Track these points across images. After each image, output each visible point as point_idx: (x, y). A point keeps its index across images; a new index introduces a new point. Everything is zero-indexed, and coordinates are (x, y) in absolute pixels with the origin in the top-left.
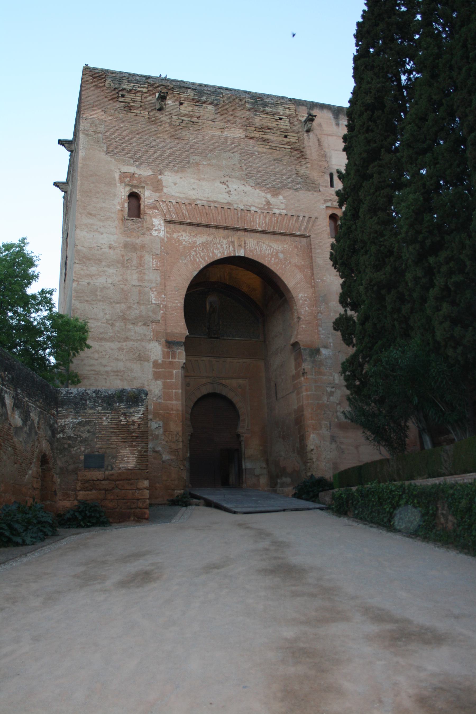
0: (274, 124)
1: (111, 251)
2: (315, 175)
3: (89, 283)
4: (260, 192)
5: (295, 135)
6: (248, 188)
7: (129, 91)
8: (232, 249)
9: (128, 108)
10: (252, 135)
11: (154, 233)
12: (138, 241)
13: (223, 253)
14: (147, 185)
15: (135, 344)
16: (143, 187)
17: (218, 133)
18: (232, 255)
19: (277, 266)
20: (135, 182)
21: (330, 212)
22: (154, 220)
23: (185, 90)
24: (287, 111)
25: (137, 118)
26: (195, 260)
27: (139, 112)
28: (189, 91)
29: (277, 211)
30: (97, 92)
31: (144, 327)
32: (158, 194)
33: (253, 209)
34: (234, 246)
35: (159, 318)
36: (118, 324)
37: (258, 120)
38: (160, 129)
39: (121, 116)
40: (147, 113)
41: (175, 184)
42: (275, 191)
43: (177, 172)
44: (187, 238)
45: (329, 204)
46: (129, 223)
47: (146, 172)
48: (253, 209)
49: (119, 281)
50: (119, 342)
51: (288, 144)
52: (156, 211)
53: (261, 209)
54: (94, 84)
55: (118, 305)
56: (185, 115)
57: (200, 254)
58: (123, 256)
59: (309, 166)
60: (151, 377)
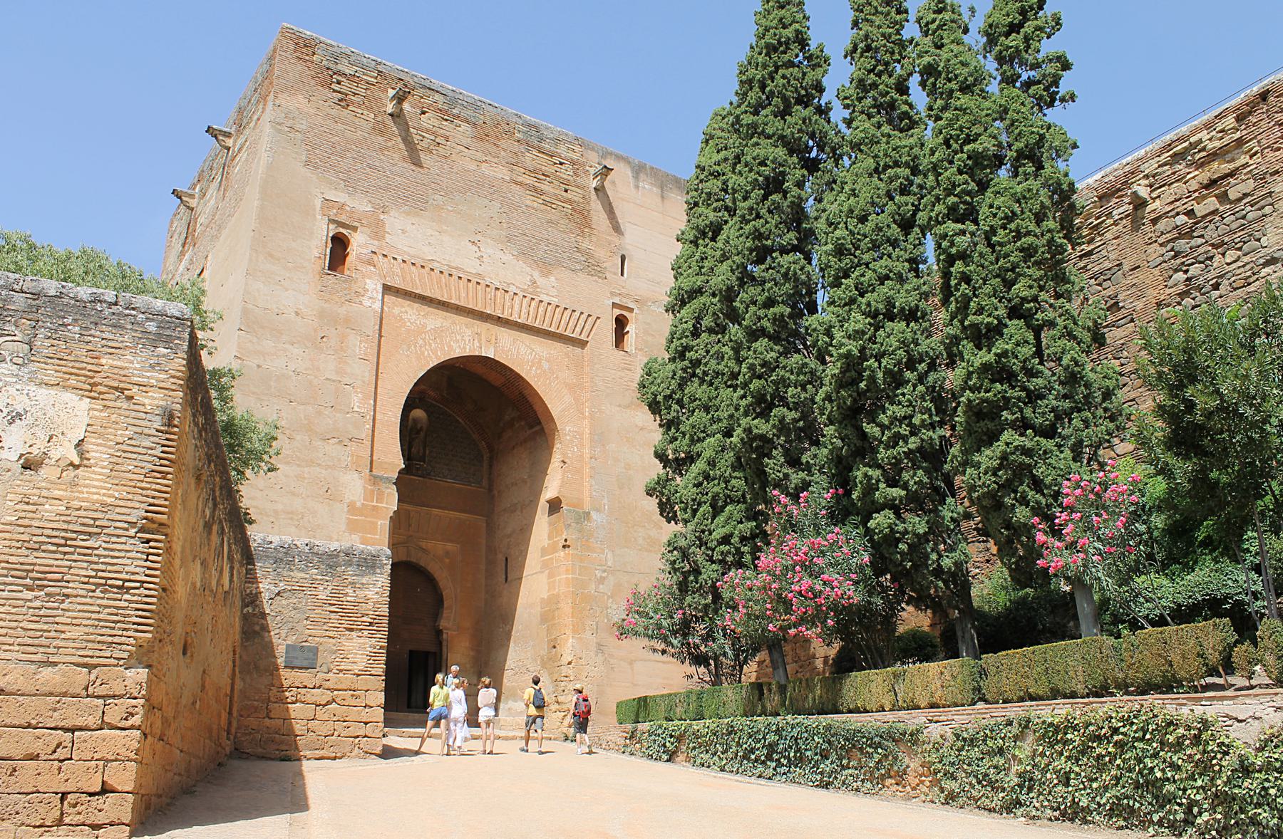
0: (550, 169)
1: (299, 319)
2: (600, 253)
3: (259, 366)
4: (524, 266)
5: (579, 191)
6: (507, 258)
7: (350, 78)
8: (477, 344)
9: (344, 102)
10: (520, 179)
11: (367, 303)
12: (342, 311)
13: (465, 348)
14: (363, 225)
15: (324, 472)
16: (355, 229)
17: (472, 166)
18: (477, 354)
19: (539, 380)
20: (343, 218)
21: (617, 312)
22: (368, 281)
23: (430, 92)
24: (571, 155)
25: (357, 120)
26: (423, 353)
27: (361, 111)
28: (437, 95)
29: (546, 299)
30: (300, 67)
31: (339, 447)
32: (376, 242)
33: (512, 289)
34: (480, 341)
35: (363, 436)
36: (298, 438)
37: (531, 159)
38: (390, 144)
39: (334, 112)
40: (373, 116)
41: (404, 232)
42: (546, 267)
43: (408, 214)
44: (414, 317)
45: (617, 300)
46: (331, 280)
47: (360, 205)
48: (512, 289)
49: (306, 370)
50: (298, 465)
51: (568, 201)
52: (372, 268)
53: (523, 290)
54: (297, 54)
55: (302, 407)
56: (427, 131)
57: (430, 345)
58: (315, 331)
59: (594, 239)
60: (343, 527)
